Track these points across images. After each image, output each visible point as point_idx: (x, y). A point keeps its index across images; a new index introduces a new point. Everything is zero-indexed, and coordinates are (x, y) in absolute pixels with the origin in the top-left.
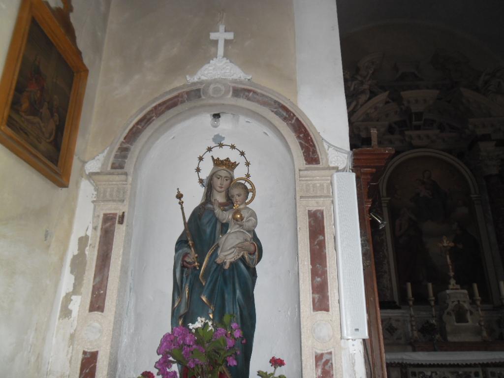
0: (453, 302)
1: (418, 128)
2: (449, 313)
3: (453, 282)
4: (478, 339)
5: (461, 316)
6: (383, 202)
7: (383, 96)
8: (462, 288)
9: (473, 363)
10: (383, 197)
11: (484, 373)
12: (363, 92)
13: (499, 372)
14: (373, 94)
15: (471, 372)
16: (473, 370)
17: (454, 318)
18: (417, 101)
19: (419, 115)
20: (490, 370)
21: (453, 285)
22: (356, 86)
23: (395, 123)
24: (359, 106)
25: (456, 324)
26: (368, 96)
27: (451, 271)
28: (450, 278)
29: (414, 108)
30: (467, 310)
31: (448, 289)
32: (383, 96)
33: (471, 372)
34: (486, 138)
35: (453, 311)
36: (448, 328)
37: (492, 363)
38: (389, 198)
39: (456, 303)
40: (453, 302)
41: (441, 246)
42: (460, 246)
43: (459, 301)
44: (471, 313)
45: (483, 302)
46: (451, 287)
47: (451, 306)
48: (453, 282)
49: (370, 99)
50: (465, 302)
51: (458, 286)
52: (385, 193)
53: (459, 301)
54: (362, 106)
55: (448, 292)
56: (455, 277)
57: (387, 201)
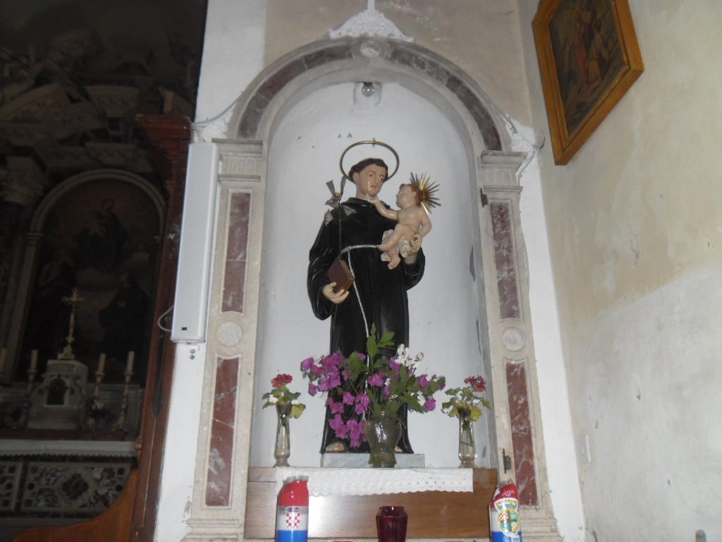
0: (52, 376)
1: (117, 140)
2: (41, 392)
3: (68, 350)
4: (71, 426)
5: (56, 394)
8: (76, 359)
9: (14, 454)
11: (25, 468)
13: (43, 467)
14: (40, 81)
15: (5, 467)
16: (9, 464)
17: (45, 396)
19: (114, 122)
20: (32, 464)
21: (66, 355)
25: (46, 406)
27: (71, 335)
28: (65, 344)
30: (67, 388)
31: (55, 358)
33: (5, 467)
35: (47, 388)
36: (34, 411)
37: (38, 455)
39: (56, 377)
40: (52, 376)
41: (85, 304)
42: (122, 305)
43: (59, 376)
44: (72, 392)
45: (105, 380)
46: (60, 356)
47: (48, 378)
48: (68, 350)
50: (67, 376)
51: (73, 356)
53: (59, 376)
55: (50, 362)
56: (73, 345)
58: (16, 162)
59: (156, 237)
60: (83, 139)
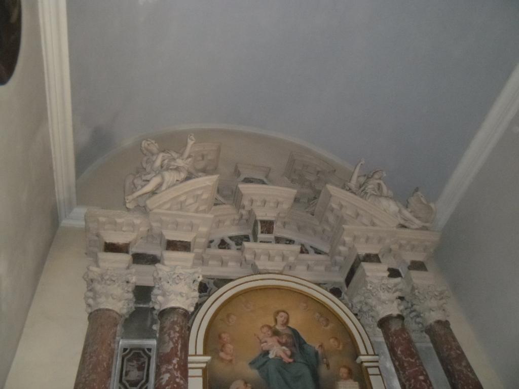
6: (190, 365)
7: (208, 182)
10: (196, 355)
12: (177, 169)
18: (265, 202)
19: (268, 226)
22: (166, 162)
23: (231, 238)
24: (164, 188)
26: (183, 175)
29: (262, 214)
32: (208, 182)
34: (372, 258)
38: (208, 358)
49: (188, 178)
52: (200, 350)
54: (169, 187)
57: (204, 365)
58: (171, 256)
59: (362, 358)
60: (223, 244)
